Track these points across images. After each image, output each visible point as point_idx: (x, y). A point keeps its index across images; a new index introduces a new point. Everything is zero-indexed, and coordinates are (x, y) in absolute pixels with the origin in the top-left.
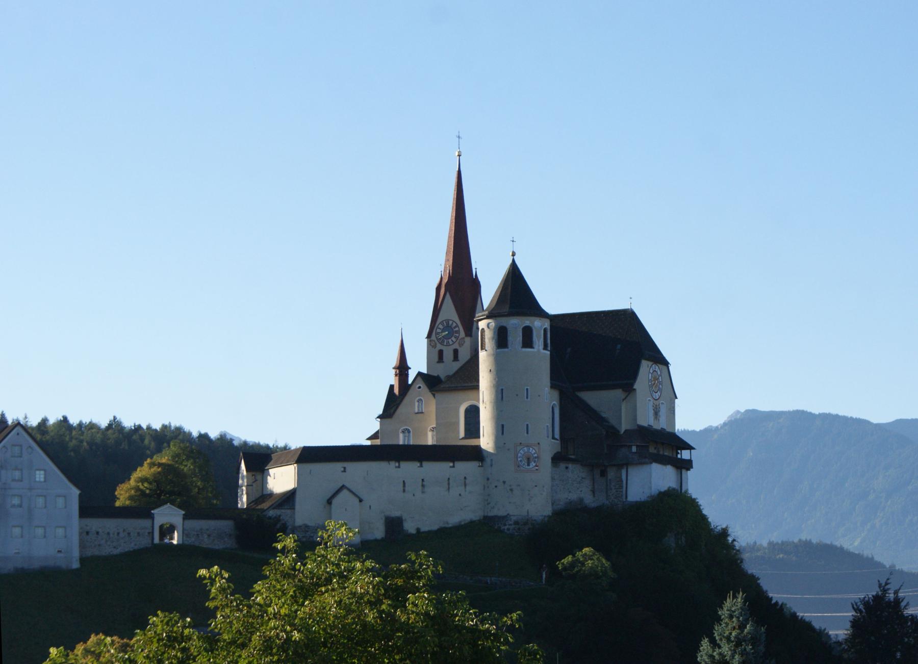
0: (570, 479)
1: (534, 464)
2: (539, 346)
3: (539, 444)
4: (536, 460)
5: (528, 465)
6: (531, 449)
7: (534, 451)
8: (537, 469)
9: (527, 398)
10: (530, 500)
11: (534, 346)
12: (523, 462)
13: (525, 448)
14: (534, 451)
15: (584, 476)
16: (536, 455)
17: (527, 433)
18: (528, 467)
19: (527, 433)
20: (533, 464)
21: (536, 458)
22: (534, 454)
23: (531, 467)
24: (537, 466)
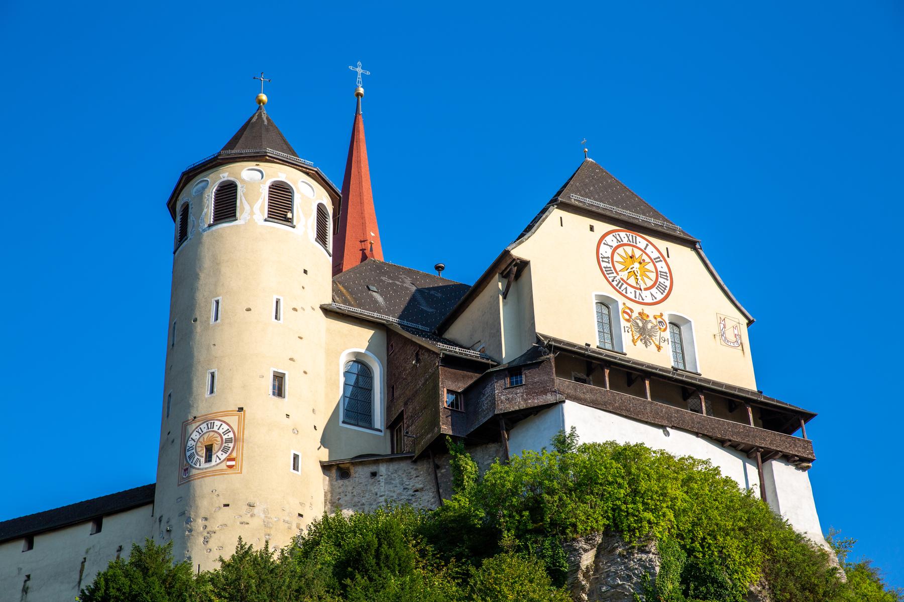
0: (382, 499)
1: (224, 456)
2: (252, 213)
3: (241, 409)
4: (231, 445)
5: (209, 459)
6: (217, 423)
7: (225, 427)
8: (230, 467)
9: (216, 319)
10: (206, 541)
11: (238, 214)
12: (197, 457)
13: (204, 426)
14: (225, 427)
15: (420, 486)
16: (231, 435)
17: (212, 392)
18: (208, 465)
19: (212, 392)
20: (219, 456)
21: (229, 441)
22: (227, 432)
23: (213, 463)
24: (233, 460)
